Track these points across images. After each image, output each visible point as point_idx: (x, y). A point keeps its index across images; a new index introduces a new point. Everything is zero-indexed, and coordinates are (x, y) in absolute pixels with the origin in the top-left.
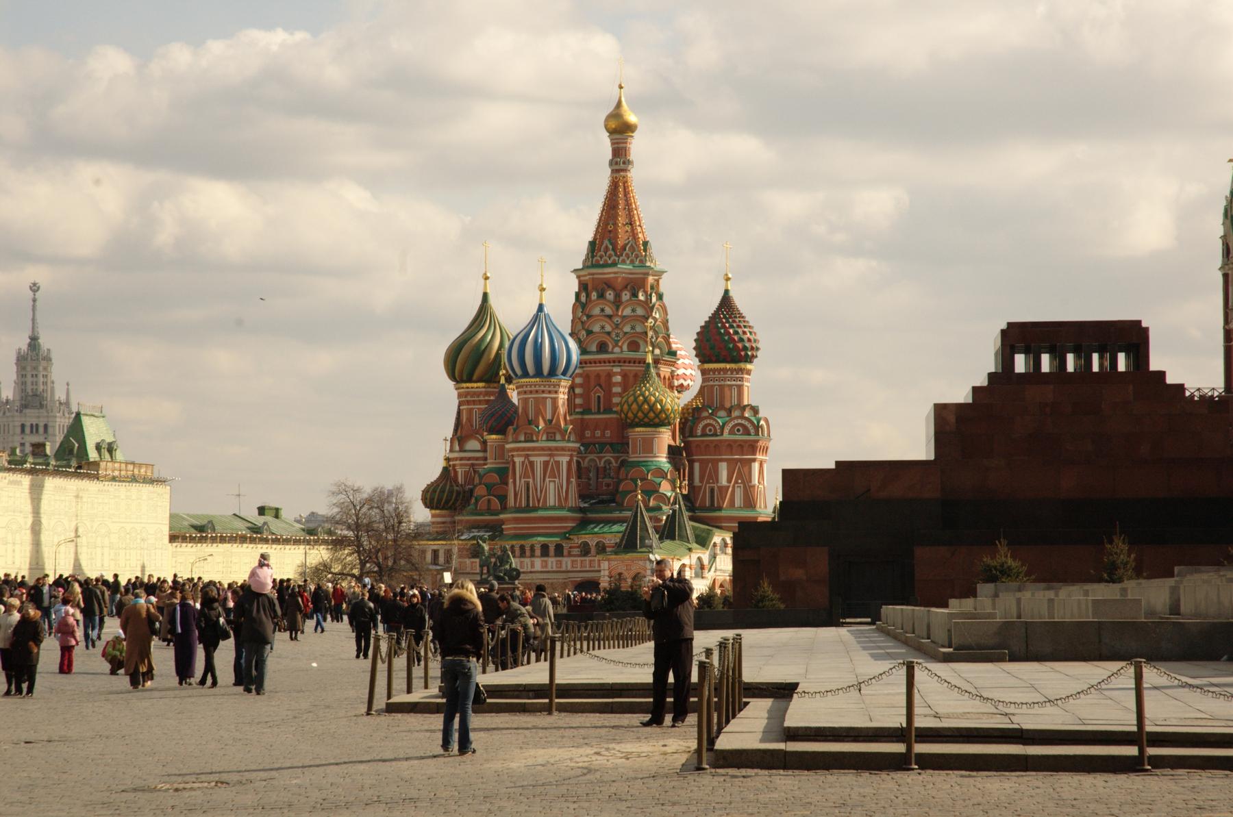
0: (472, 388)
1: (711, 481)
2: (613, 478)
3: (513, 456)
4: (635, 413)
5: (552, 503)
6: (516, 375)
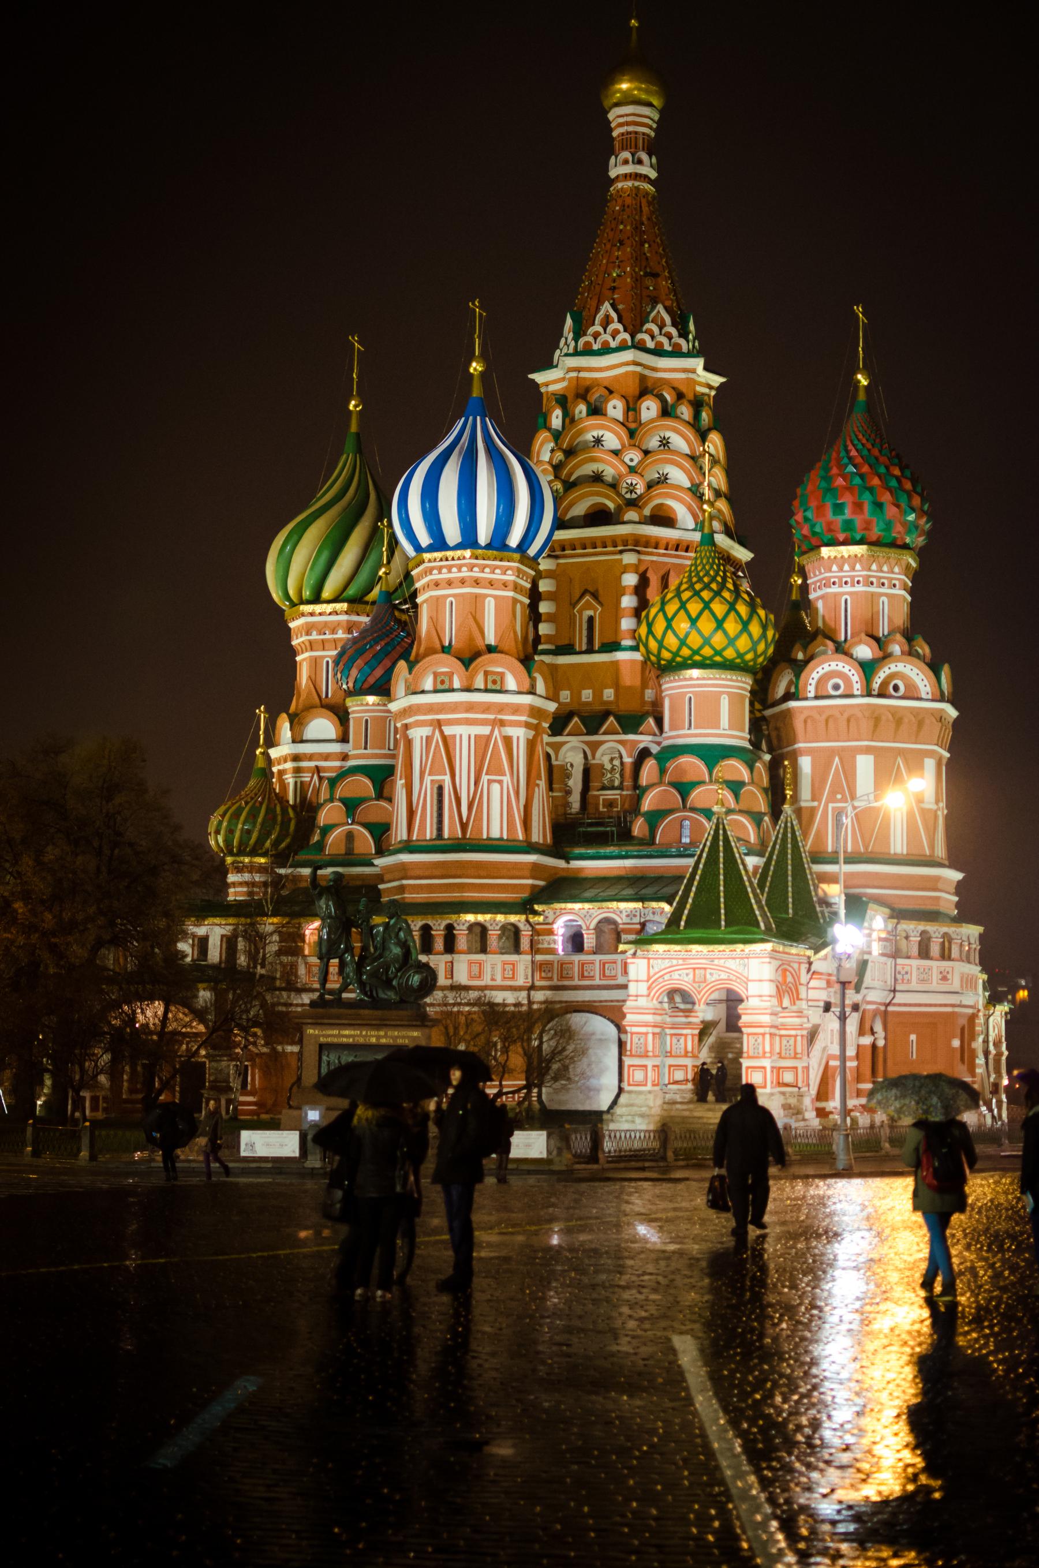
0: (320, 614)
1: (839, 796)
2: (621, 787)
3: (406, 727)
4: (682, 636)
5: (495, 833)
6: (418, 548)
